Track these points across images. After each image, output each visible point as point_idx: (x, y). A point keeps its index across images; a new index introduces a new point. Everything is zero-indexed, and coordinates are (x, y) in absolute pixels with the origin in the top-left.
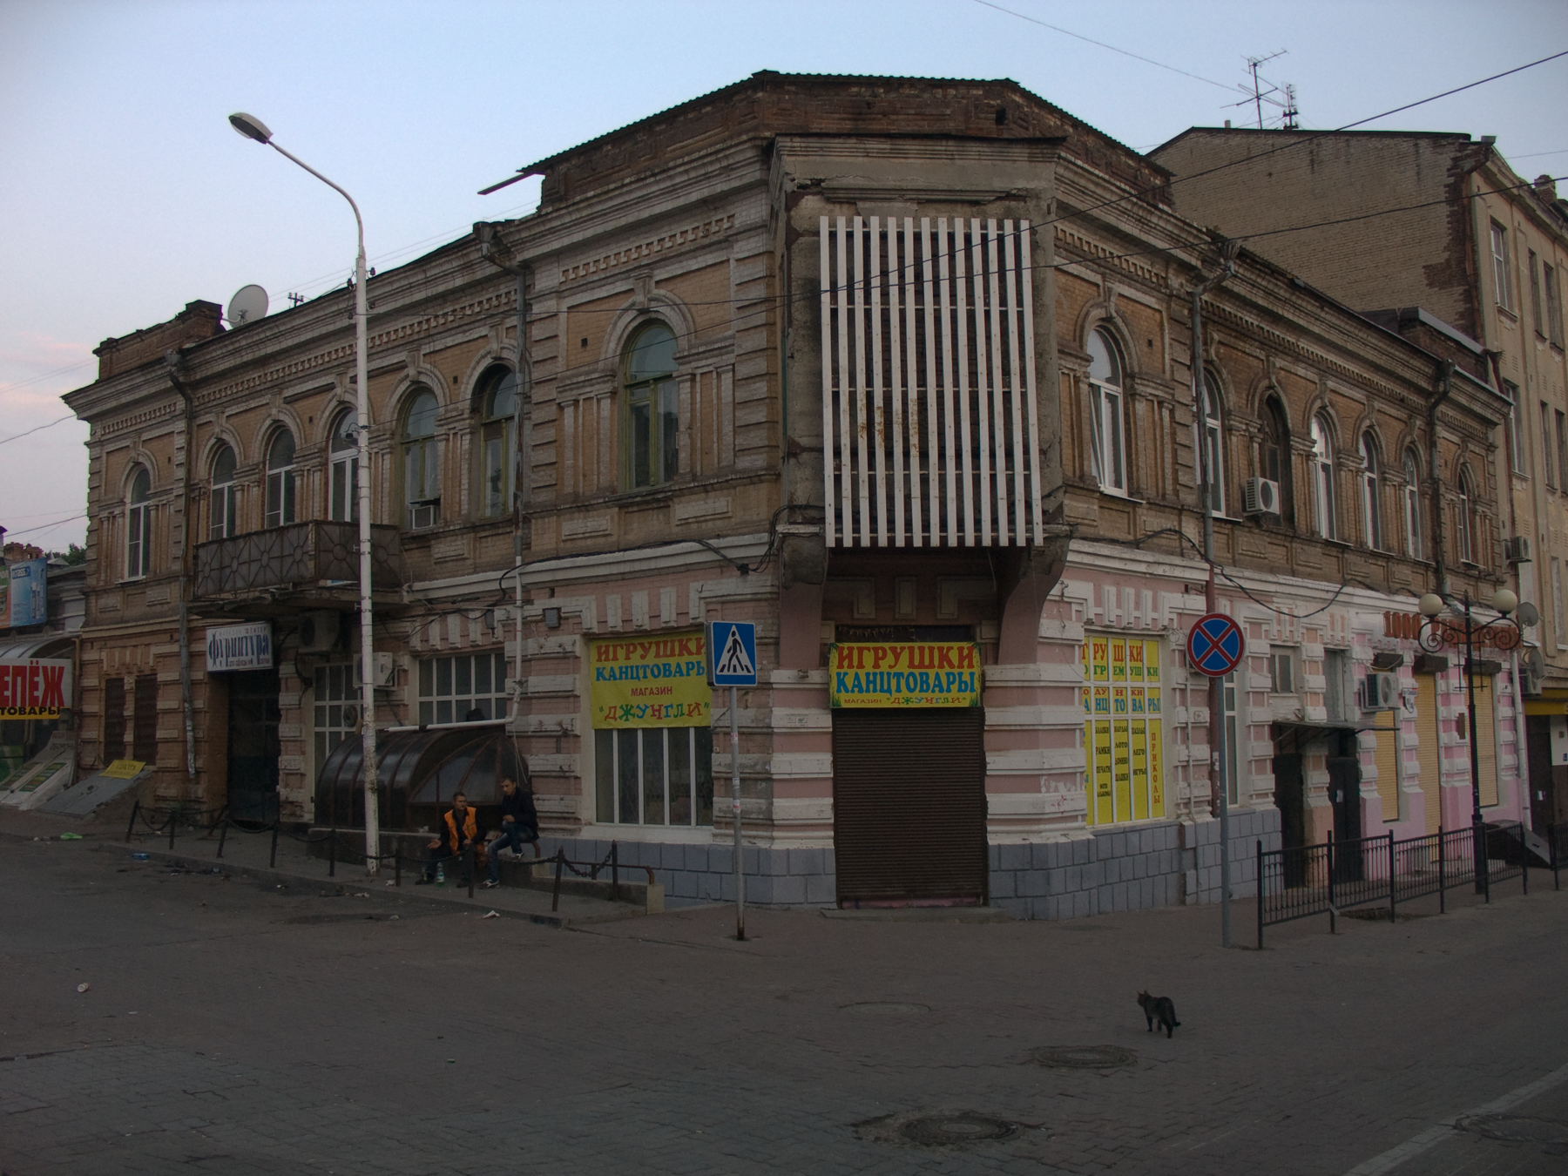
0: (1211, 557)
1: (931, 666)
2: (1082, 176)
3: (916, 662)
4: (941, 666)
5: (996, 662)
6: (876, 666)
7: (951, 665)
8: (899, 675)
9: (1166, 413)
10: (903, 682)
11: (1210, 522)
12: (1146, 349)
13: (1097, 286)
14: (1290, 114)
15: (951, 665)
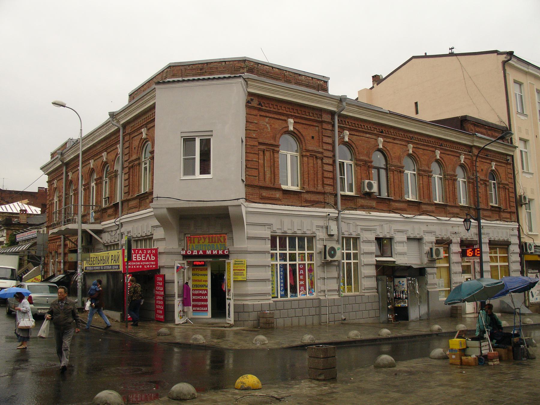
1: (215, 242)
4: (218, 242)
6: (199, 242)
7: (221, 242)
8: (205, 245)
14: (452, 48)
15: (221, 242)
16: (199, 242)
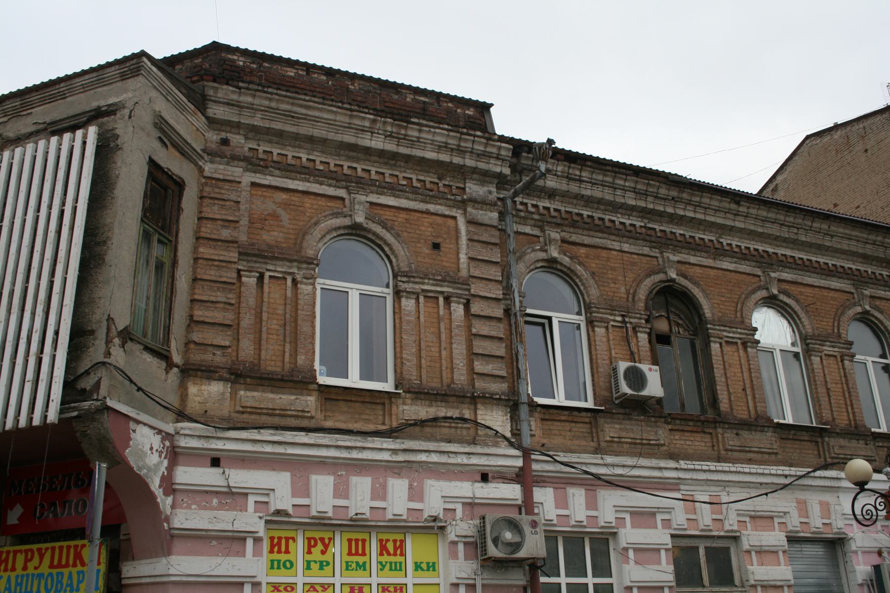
0: (527, 442)
1: (67, 565)
2: (283, 102)
3: (56, 563)
4: (75, 565)
5: (133, 559)
6: (25, 568)
8: (41, 576)
9: (458, 310)
10: (43, 582)
11: (524, 410)
12: (426, 250)
13: (343, 199)
16: (25, 568)
